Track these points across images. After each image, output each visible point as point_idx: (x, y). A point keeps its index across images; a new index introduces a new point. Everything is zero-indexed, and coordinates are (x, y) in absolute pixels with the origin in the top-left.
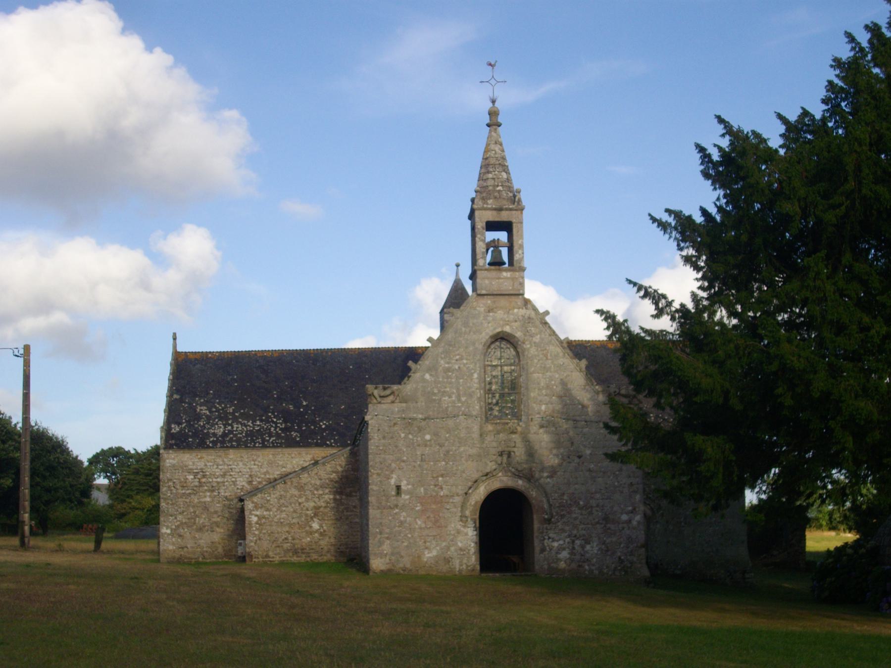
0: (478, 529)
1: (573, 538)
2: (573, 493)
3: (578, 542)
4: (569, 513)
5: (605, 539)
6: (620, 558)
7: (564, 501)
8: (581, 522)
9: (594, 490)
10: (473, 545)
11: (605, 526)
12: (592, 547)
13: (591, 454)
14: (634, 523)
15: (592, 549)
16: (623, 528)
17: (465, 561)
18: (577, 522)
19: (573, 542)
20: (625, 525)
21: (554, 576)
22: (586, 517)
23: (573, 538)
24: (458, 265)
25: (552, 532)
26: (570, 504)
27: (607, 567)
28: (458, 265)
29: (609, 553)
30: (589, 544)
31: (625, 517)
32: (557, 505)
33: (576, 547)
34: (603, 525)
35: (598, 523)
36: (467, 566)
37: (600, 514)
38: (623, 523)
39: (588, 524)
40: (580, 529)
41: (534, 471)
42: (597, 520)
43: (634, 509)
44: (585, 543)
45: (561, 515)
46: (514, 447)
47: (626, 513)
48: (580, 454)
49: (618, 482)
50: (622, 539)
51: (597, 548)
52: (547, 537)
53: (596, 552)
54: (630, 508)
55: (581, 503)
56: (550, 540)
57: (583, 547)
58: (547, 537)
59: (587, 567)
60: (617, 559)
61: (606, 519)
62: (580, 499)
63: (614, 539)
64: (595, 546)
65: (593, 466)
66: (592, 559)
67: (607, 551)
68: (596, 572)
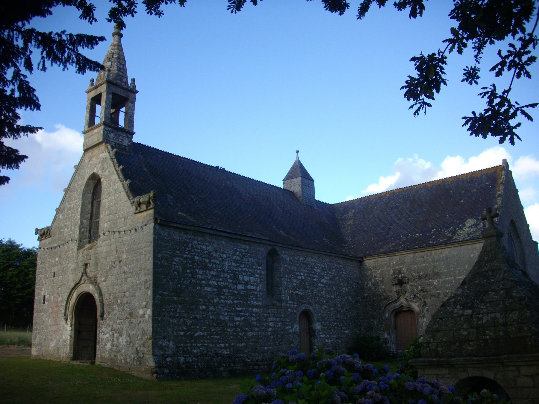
0: (73, 326)
1: (114, 332)
2: (115, 293)
3: (116, 335)
4: (113, 310)
5: (130, 332)
6: (137, 349)
7: (111, 300)
8: (118, 318)
9: (126, 289)
10: (69, 337)
11: (130, 321)
12: (122, 339)
13: (126, 258)
14: (147, 316)
15: (123, 341)
16: (140, 322)
17: (65, 350)
18: (116, 318)
19: (113, 335)
20: (141, 319)
21: (103, 364)
22: (120, 312)
23: (114, 332)
24: (297, 152)
25: (104, 326)
26: (113, 303)
27: (129, 357)
28: (297, 152)
29: (131, 345)
30: (121, 336)
31: (141, 312)
32: (107, 304)
33: (114, 339)
34: (129, 320)
35: (127, 318)
36: (66, 354)
37: (128, 310)
38: (140, 317)
39: (121, 319)
40: (117, 324)
41: (97, 277)
42: (126, 315)
43: (147, 304)
44: (119, 336)
45: (109, 312)
46: (90, 259)
47: (142, 308)
48: (120, 259)
49: (139, 280)
50: (139, 332)
51: (125, 340)
52: (101, 331)
53: (124, 343)
54: (145, 303)
55: (119, 301)
56: (103, 333)
57: (118, 339)
58: (101, 331)
59: (119, 357)
60: (135, 350)
61: (131, 314)
62: (118, 298)
63: (135, 332)
64: (124, 338)
65: (126, 268)
66: (122, 350)
67: (130, 342)
68: (123, 361)
